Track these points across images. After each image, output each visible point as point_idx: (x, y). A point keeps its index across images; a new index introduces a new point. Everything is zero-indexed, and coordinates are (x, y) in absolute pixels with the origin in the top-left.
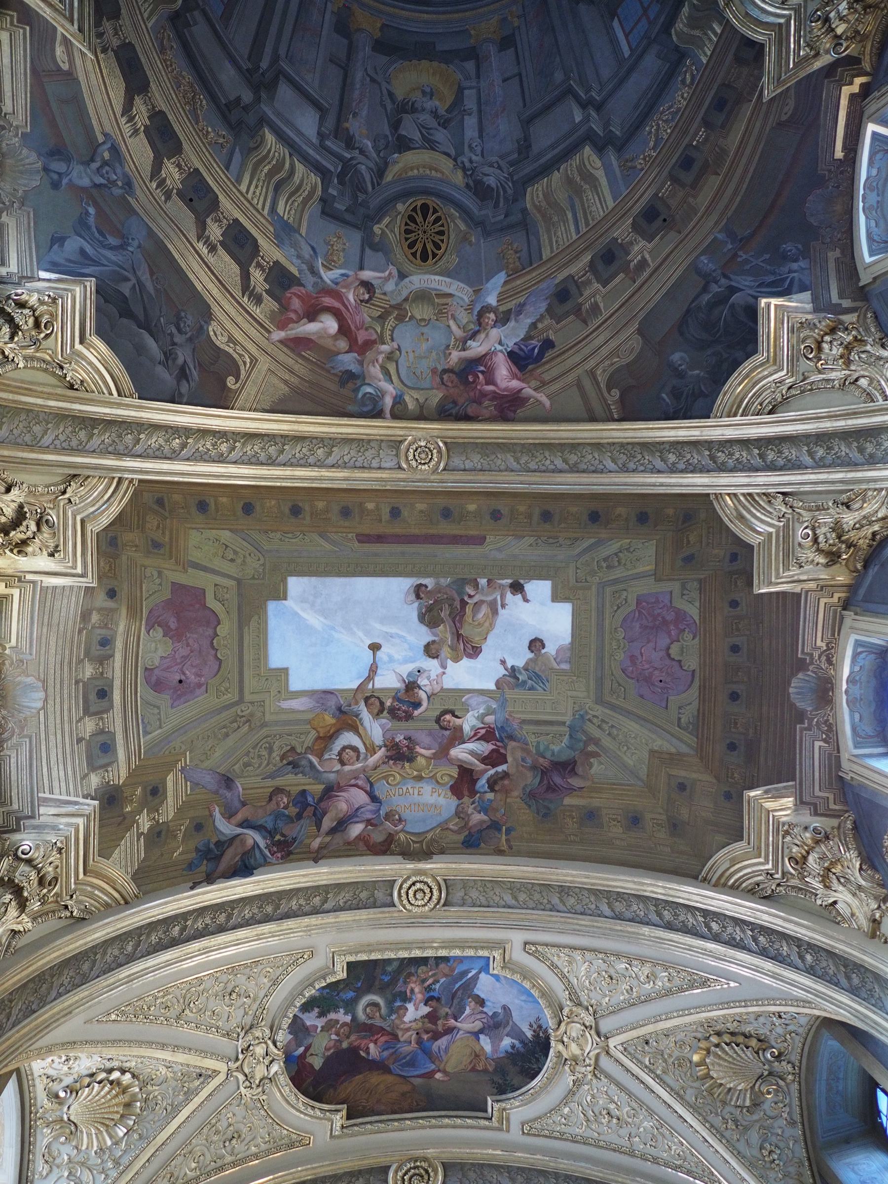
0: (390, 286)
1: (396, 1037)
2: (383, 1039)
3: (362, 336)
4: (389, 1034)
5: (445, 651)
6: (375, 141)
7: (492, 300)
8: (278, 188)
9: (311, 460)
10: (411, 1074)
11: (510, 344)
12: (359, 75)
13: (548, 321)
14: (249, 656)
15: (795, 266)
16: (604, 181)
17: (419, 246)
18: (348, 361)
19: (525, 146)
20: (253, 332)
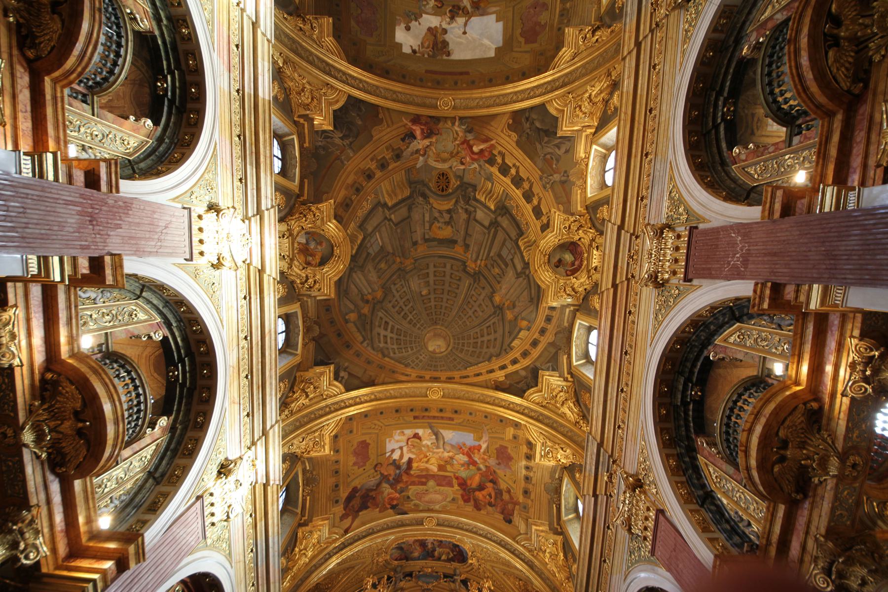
0: (455, 164)
3: (465, 146)
5: (440, 31)
6: (458, 212)
7: (421, 158)
8: (491, 191)
9: (484, 100)
11: (415, 142)
12: (462, 233)
13: (403, 148)
14: (510, 24)
15: (320, 144)
16: (385, 192)
17: (445, 178)
18: (470, 137)
19: (410, 209)
20: (502, 141)
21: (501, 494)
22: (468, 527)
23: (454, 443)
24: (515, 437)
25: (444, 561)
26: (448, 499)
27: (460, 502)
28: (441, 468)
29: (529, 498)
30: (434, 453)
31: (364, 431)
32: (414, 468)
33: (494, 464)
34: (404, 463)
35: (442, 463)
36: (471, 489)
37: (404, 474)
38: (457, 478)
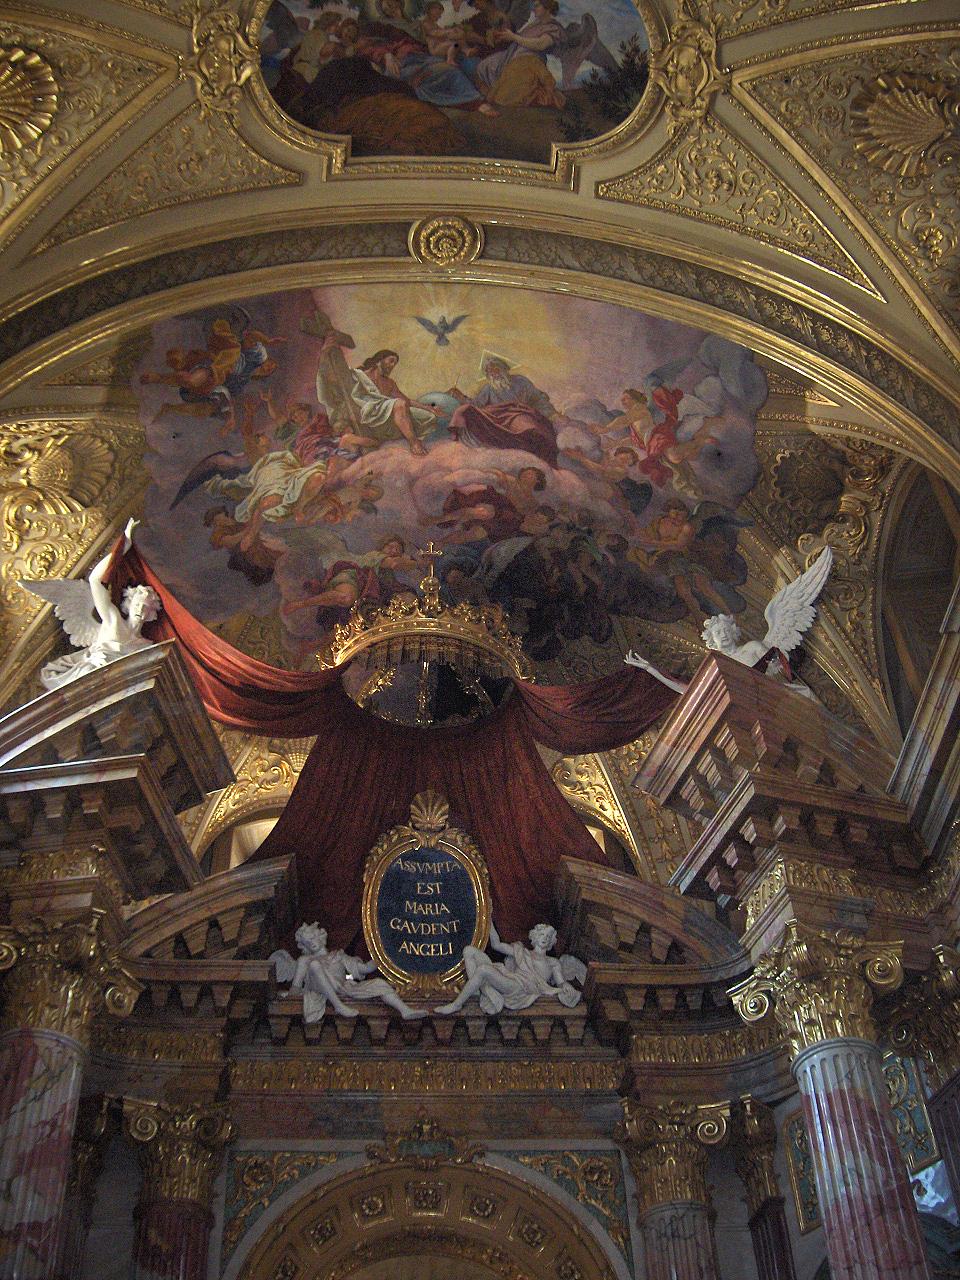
1: (424, 47)
2: (406, 49)
4: (415, 42)
10: (447, 103)
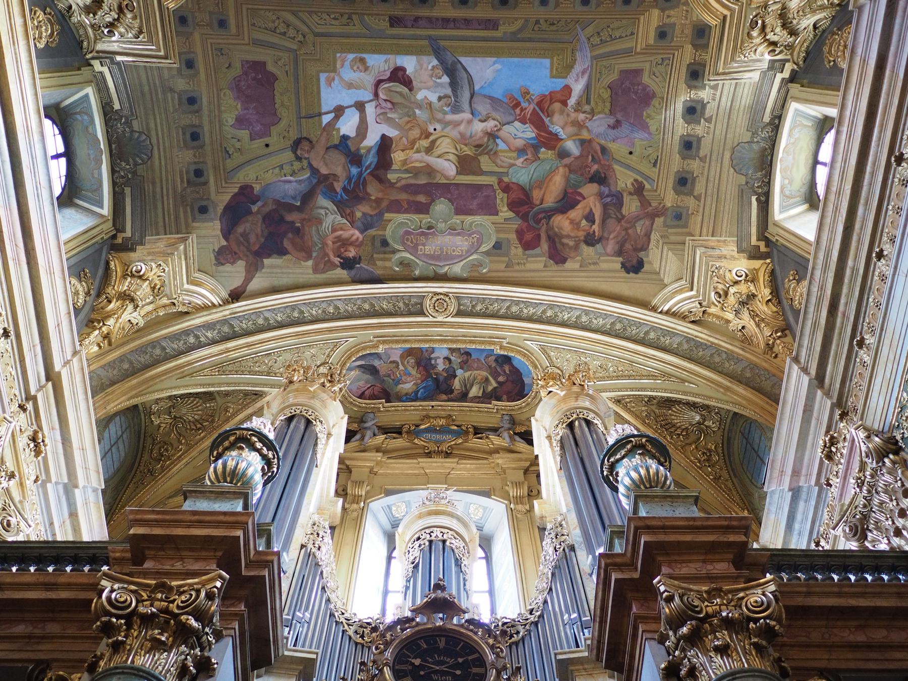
21: (619, 204)
22: (532, 311)
23: (498, 93)
24: (662, 34)
25: (476, 399)
26: (485, 248)
27: (513, 251)
28: (466, 164)
29: (690, 193)
30: (447, 124)
31: (257, 35)
32: (394, 167)
33: (602, 129)
34: (369, 150)
35: (468, 151)
36: (545, 211)
37: (370, 179)
38: (506, 188)
